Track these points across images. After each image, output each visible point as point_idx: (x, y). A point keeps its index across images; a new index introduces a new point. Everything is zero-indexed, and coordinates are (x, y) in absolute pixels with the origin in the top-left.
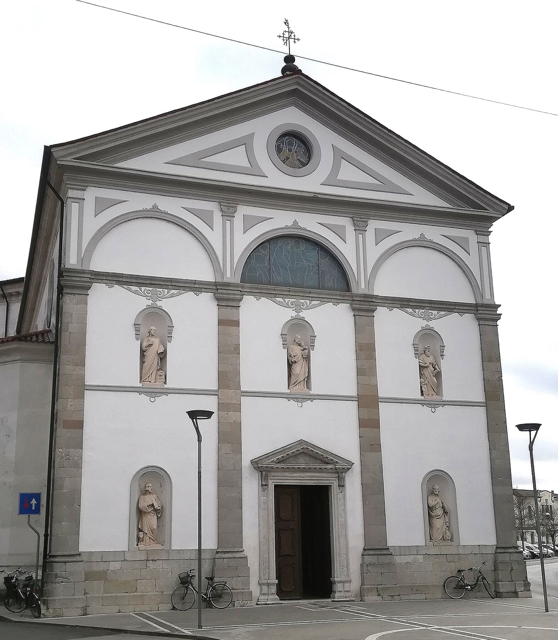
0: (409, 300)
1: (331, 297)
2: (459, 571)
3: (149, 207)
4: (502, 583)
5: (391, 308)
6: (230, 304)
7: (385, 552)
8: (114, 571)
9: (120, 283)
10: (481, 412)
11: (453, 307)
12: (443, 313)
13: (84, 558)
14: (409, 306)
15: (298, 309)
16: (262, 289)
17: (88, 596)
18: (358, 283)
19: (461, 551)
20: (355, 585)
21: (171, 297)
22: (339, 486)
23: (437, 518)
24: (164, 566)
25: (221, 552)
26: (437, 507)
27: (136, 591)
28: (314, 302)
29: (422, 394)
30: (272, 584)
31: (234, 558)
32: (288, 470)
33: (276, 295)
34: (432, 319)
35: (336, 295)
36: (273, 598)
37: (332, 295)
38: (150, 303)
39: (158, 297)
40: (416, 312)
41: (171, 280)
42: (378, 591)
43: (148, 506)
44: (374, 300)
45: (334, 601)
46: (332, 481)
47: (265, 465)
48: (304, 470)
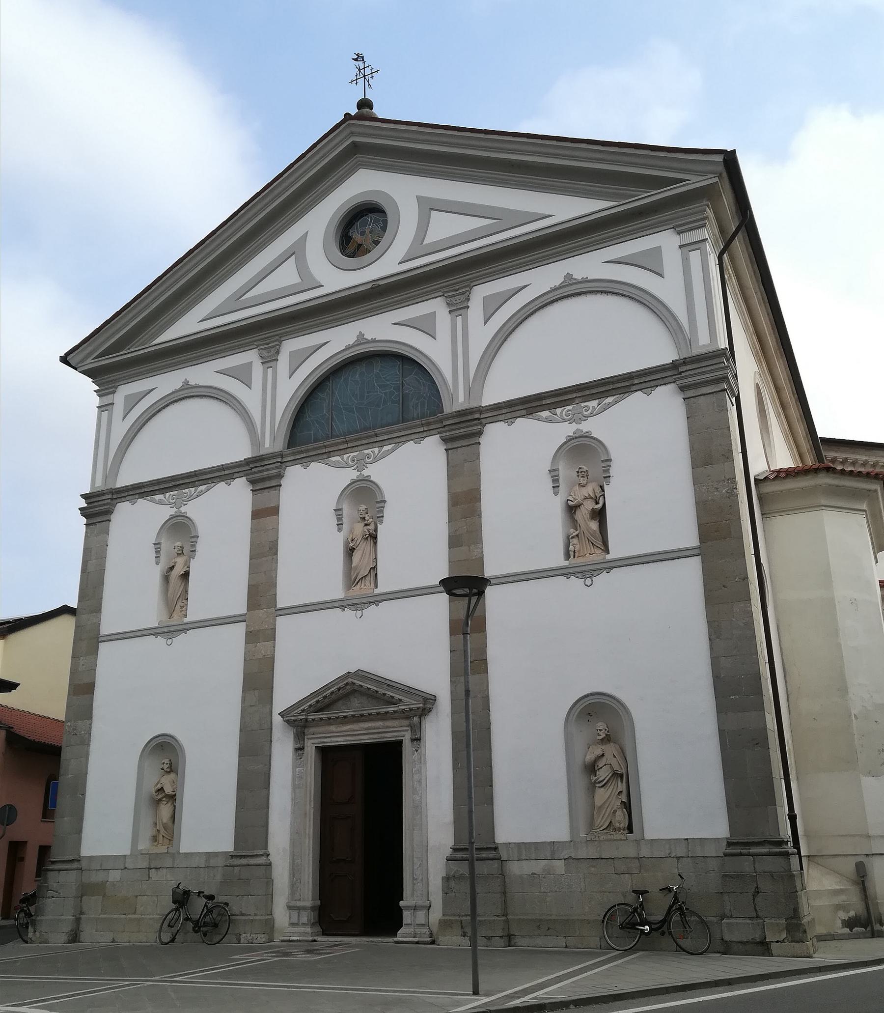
0: (539, 397)
1: (409, 432)
2: (638, 893)
3: (178, 385)
4: (732, 921)
5: (510, 420)
6: (267, 484)
7: (491, 854)
8: (113, 884)
9: (143, 495)
10: (693, 568)
11: (627, 384)
12: (610, 400)
13: (84, 864)
14: (543, 408)
15: (360, 464)
16: (307, 451)
17: (83, 916)
18: (453, 398)
19: (645, 852)
20: (436, 915)
21: (198, 496)
22: (413, 740)
23: (599, 787)
24: (168, 876)
25: (236, 856)
26: (600, 766)
27: (135, 913)
28: (385, 448)
29: (567, 556)
30: (304, 908)
31: (248, 865)
32: (329, 721)
33: (329, 454)
34: (585, 417)
35: (416, 427)
36: (305, 932)
37: (410, 428)
38: (173, 511)
39: (182, 502)
40: (556, 414)
41: (195, 474)
42: (462, 927)
43: (156, 792)
44: (477, 416)
45: (396, 942)
46: (403, 733)
47: (293, 718)
48: (361, 718)
